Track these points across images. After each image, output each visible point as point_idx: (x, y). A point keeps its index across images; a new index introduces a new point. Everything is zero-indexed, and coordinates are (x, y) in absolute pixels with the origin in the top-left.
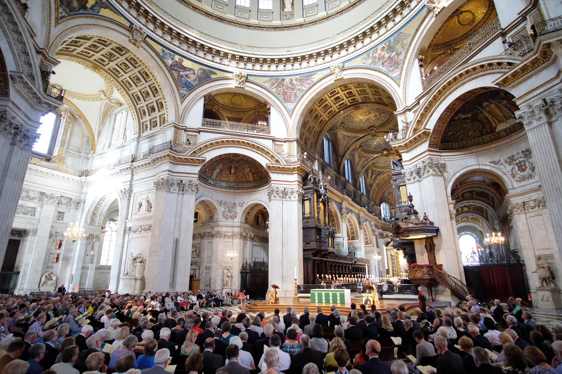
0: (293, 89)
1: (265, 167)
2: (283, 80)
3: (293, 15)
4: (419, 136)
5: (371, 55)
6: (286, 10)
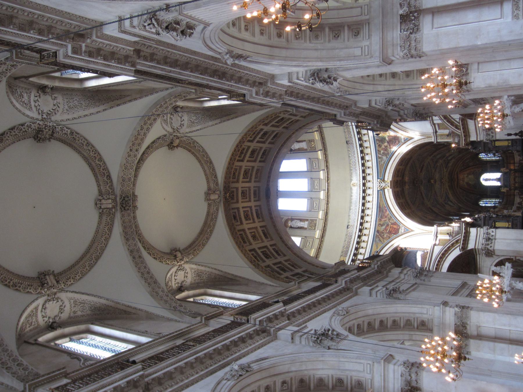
0: (388, 225)
1: (461, 252)
2: (378, 231)
3: (312, 220)
4: (462, 125)
6: (306, 226)
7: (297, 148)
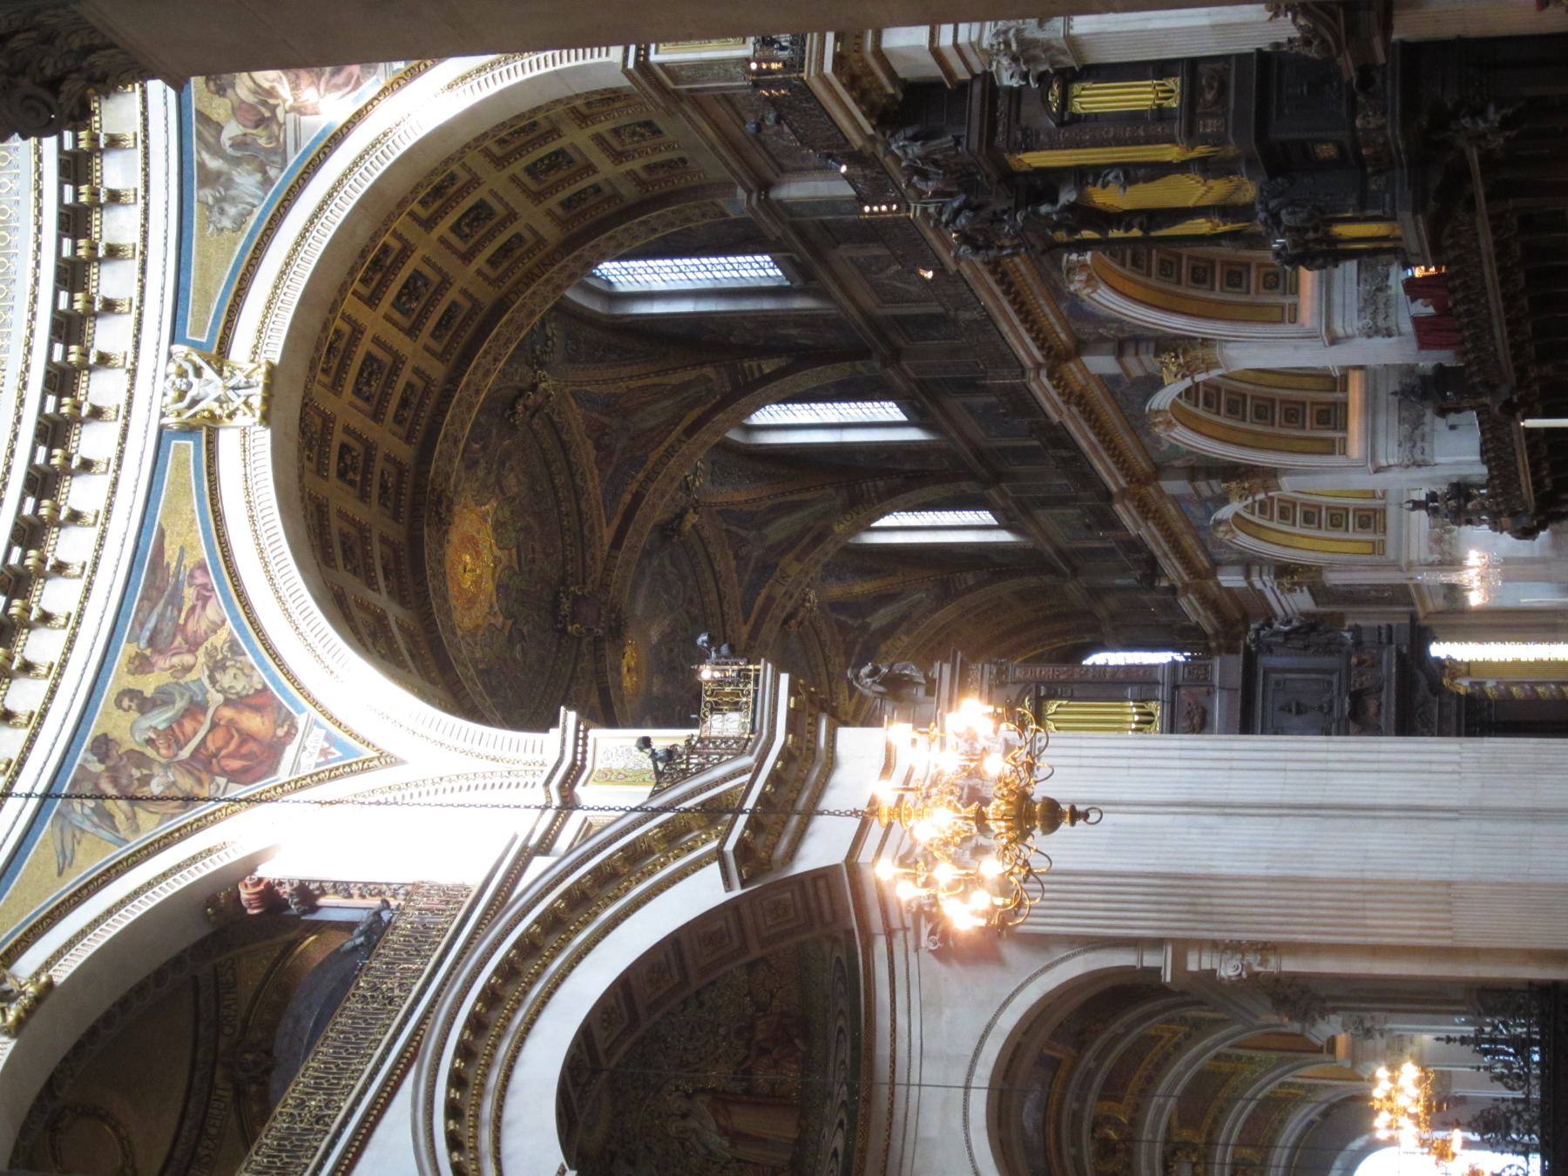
0: (196, 708)
1: (738, 891)
5: (213, 164)
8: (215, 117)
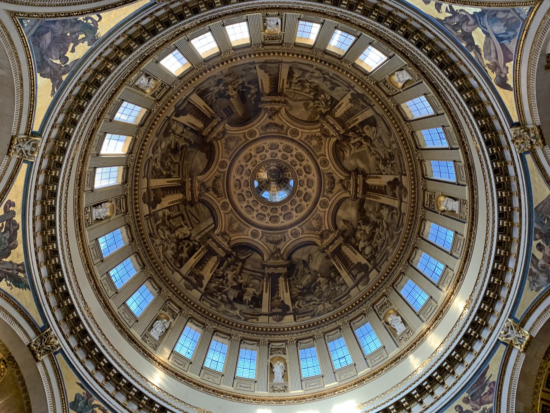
5: (534, 270)
7: (450, 209)
8: (537, 257)
